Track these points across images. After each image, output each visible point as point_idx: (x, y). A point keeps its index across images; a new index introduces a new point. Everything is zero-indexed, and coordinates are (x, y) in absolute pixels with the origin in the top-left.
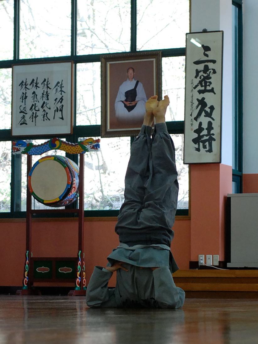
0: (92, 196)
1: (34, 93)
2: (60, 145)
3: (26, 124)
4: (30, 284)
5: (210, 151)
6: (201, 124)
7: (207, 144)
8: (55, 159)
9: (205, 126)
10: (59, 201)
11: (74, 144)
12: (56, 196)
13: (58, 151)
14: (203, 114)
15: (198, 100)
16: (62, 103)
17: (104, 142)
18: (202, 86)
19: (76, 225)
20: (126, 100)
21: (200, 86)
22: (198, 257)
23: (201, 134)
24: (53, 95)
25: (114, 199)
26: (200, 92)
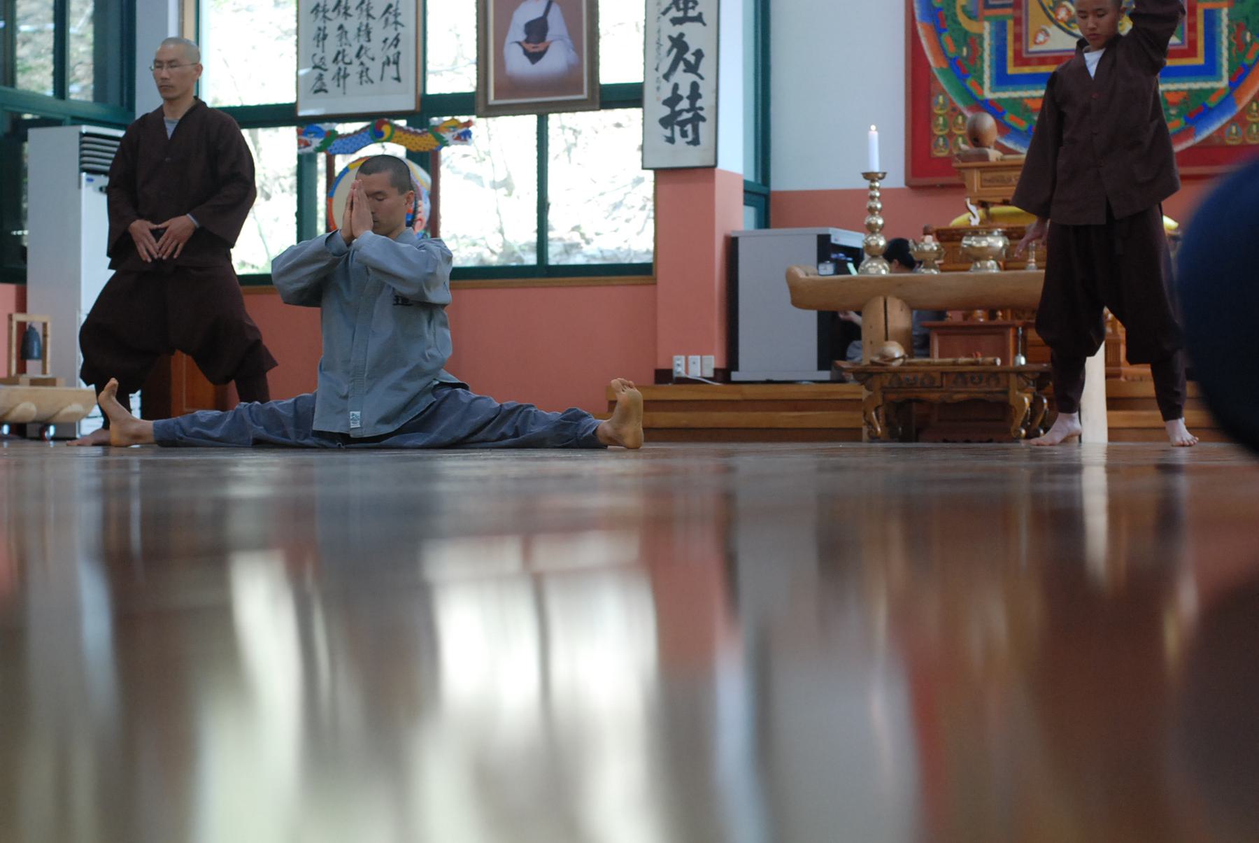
0: (483, 242)
1: (341, 27)
2: (393, 132)
3: (326, 91)
5: (695, 142)
6: (676, 87)
7: (689, 128)
9: (684, 91)
11: (419, 131)
13: (387, 144)
14: (682, 66)
15: (670, 38)
16: (400, 48)
17: (480, 126)
18: (678, 9)
20: (527, 41)
21: (674, 10)
22: (671, 360)
23: (678, 108)
25: (526, 248)
26: (675, 21)
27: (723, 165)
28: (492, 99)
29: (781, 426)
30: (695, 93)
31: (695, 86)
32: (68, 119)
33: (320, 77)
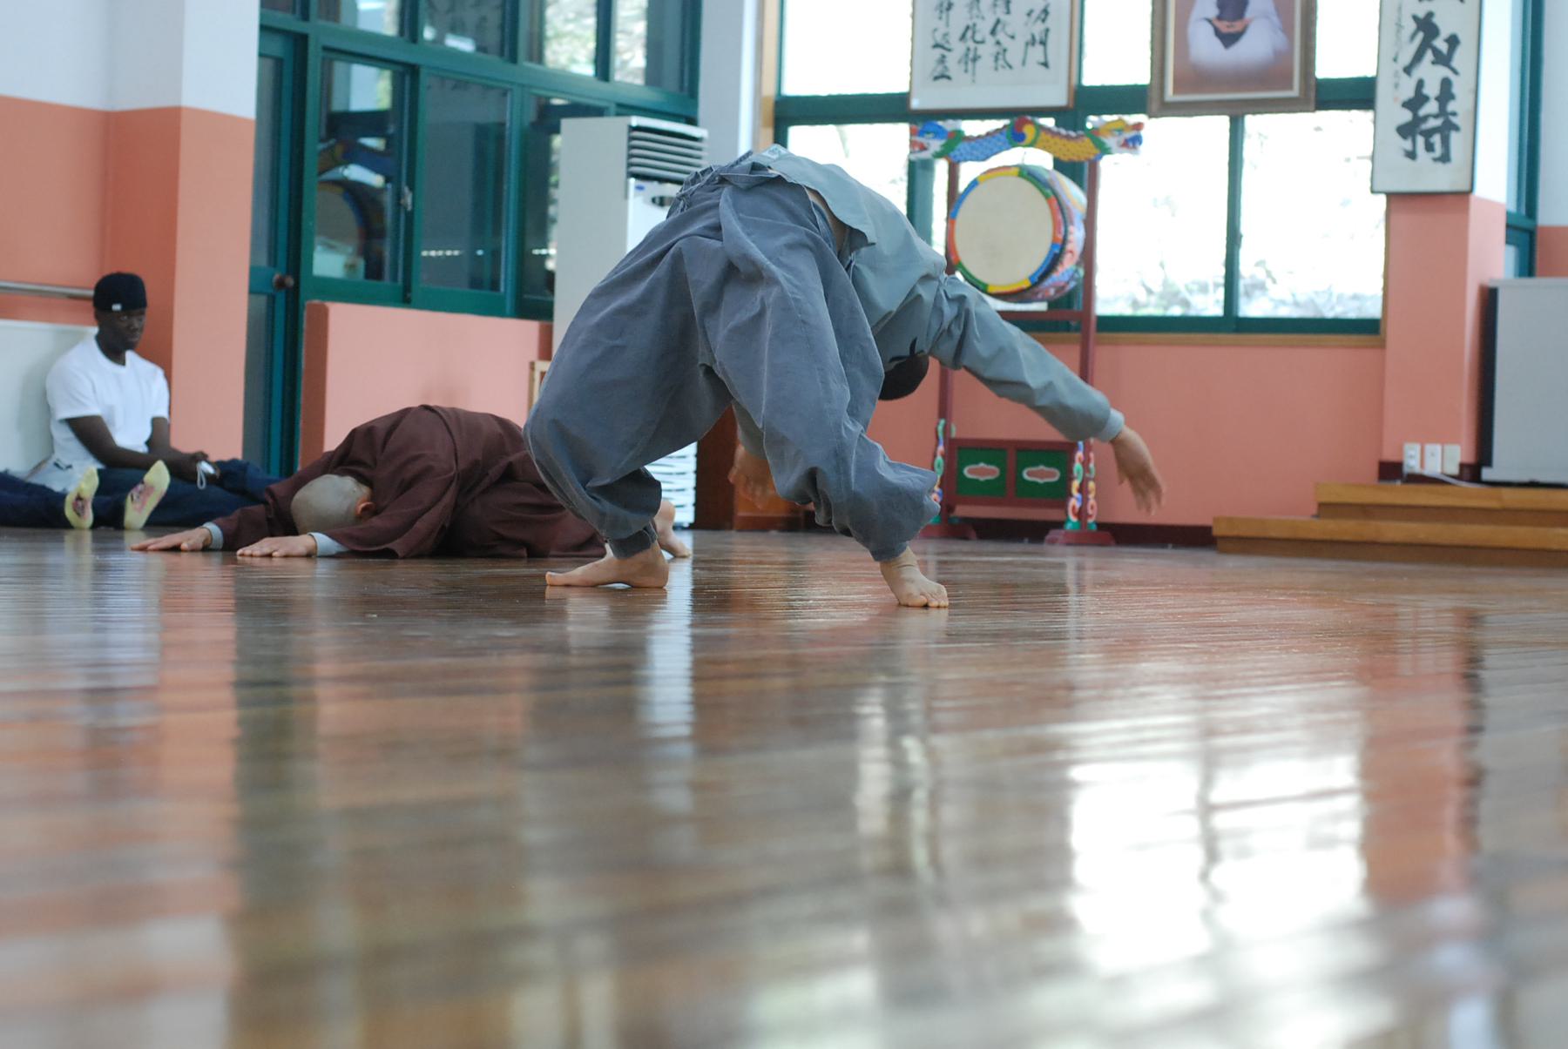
2: (1038, 135)
4: (947, 507)
5: (1445, 158)
6: (1420, 84)
7: (1436, 139)
8: (1021, 175)
9: (1432, 90)
10: (1029, 289)
11: (1072, 134)
12: (1019, 274)
14: (1429, 56)
15: (1415, 18)
16: (1049, 23)
17: (1155, 129)
20: (1219, 18)
25: (1195, 287)
27: (1480, 191)
28: (1170, 95)
29: (1555, 547)
30: (1446, 94)
31: (1446, 84)
32: (613, 108)
33: (942, 60)
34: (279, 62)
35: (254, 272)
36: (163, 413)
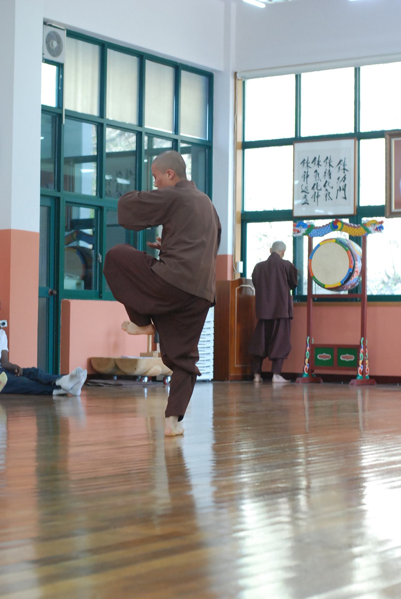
1: (316, 171)
3: (308, 204)
4: (311, 371)
11: (356, 225)
12: (337, 281)
16: (346, 182)
19: (359, 310)
24: (336, 173)
28: (393, 209)
33: (305, 196)
34: (49, 208)
35: (40, 289)
36: (6, 349)
